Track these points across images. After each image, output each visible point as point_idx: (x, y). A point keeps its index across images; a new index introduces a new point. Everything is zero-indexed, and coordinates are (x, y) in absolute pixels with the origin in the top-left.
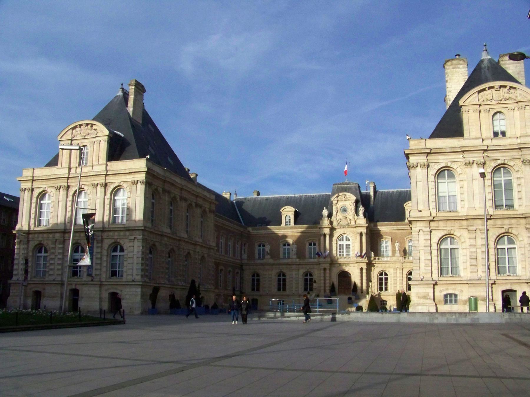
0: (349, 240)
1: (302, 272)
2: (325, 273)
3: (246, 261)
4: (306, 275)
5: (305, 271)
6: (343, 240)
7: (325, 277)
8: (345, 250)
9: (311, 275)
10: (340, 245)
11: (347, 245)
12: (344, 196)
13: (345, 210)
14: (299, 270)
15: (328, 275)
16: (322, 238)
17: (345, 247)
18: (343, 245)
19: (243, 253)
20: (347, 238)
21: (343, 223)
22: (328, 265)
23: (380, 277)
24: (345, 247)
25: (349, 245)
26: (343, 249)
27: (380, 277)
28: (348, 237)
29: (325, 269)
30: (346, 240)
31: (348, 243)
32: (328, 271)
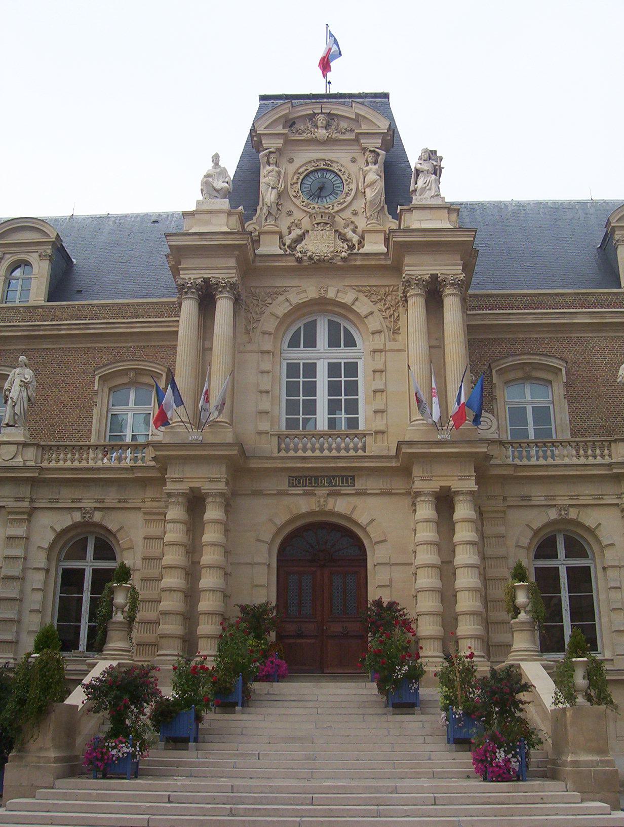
0: (351, 342)
1: (48, 526)
5: (64, 521)
6: (311, 342)
7: (193, 549)
8: (322, 397)
10: (293, 370)
11: (334, 369)
12: (321, 120)
14: (31, 513)
15: (211, 535)
17: (322, 380)
18: (311, 370)
20: (334, 328)
21: (319, 244)
22: (220, 472)
23: (542, 563)
24: (322, 380)
25: (352, 369)
26: (311, 389)
27: (542, 563)
28: (344, 323)
29: (195, 503)
30: (333, 342)
31: (342, 355)
32: (213, 513)
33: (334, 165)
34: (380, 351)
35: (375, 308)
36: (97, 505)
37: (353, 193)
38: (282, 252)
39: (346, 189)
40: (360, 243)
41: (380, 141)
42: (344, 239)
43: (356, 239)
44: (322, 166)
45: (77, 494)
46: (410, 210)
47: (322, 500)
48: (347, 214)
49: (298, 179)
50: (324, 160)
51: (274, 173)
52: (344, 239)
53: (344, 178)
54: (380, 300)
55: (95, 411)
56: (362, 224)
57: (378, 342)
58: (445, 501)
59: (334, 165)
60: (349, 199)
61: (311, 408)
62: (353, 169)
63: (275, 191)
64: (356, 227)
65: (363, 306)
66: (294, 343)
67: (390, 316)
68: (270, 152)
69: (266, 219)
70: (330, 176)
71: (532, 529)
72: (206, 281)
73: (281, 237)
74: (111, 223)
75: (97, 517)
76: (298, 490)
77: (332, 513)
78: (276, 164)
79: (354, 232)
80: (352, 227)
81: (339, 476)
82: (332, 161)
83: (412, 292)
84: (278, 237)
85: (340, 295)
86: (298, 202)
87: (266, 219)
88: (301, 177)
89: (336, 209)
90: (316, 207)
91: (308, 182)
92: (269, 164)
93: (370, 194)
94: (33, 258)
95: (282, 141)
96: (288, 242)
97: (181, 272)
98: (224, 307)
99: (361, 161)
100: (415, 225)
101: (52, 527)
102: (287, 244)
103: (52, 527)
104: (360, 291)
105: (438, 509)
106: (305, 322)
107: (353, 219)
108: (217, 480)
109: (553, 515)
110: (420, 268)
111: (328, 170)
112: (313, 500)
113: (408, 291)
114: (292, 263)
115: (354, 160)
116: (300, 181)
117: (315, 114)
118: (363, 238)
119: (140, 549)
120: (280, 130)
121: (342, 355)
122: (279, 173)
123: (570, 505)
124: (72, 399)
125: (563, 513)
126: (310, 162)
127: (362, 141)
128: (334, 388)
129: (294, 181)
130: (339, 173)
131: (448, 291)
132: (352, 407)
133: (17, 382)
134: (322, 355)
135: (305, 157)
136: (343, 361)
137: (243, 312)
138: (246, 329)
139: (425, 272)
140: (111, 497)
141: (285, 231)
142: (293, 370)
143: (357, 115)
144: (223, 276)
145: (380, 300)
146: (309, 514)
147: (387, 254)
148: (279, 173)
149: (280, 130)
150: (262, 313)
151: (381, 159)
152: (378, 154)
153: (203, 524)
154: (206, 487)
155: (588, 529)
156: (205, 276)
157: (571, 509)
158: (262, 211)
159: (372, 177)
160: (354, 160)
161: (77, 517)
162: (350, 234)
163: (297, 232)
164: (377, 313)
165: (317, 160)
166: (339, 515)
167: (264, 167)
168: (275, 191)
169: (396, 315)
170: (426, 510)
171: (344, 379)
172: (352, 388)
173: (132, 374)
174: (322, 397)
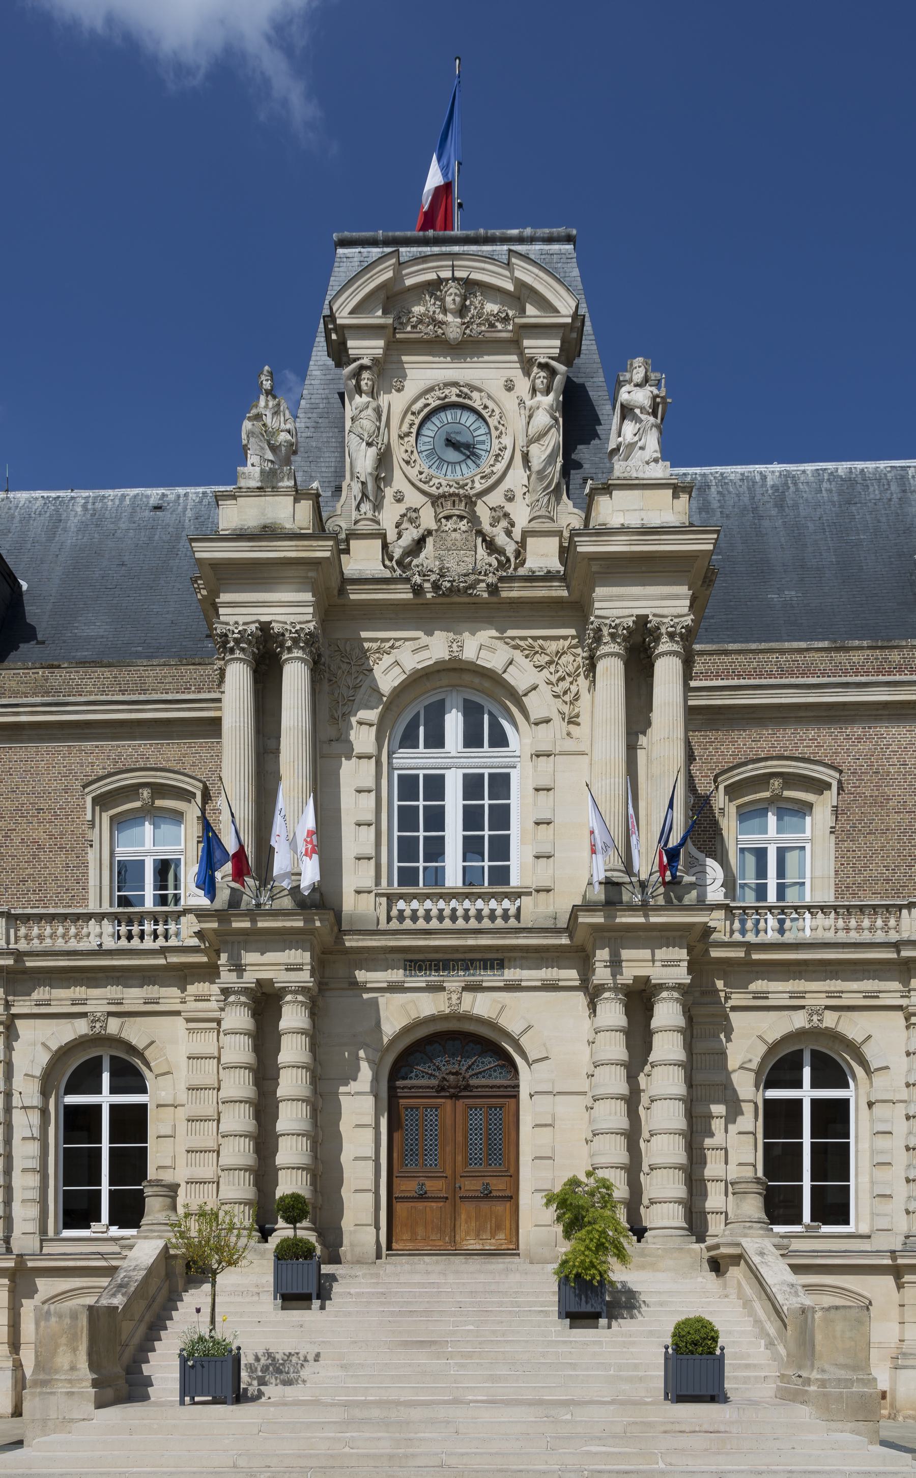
0: (499, 739)
4: (85, 1079)
5: (65, 1033)
6: (436, 740)
8: (454, 833)
9: (129, 1076)
10: (408, 786)
11: (472, 785)
17: (454, 803)
18: (436, 786)
20: (472, 713)
24: (454, 803)
25: (501, 784)
26: (436, 819)
30: (472, 739)
31: (485, 761)
33: (475, 395)
35: (540, 678)
36: (113, 1008)
37: (507, 454)
38: (387, 574)
40: (518, 554)
41: (558, 343)
42: (491, 546)
44: (454, 399)
45: (79, 992)
46: (607, 489)
47: (454, 997)
48: (496, 498)
49: (411, 425)
50: (455, 384)
51: (370, 411)
52: (491, 546)
53: (493, 422)
54: (550, 663)
55: (92, 856)
56: (521, 514)
58: (640, 999)
59: (475, 395)
60: (500, 467)
61: (436, 850)
63: (373, 451)
64: (513, 525)
65: (521, 675)
66: (409, 740)
67: (565, 693)
68: (362, 368)
69: (358, 508)
70: (468, 419)
71: (765, 1042)
73: (385, 546)
74: (79, 509)
75: (113, 1026)
76: (419, 980)
78: (373, 394)
79: (509, 533)
80: (504, 523)
81: (480, 960)
82: (473, 388)
83: (604, 649)
84: (379, 542)
85: (483, 653)
86: (412, 473)
87: (358, 508)
88: (417, 422)
89: (479, 487)
90: (444, 483)
91: (429, 430)
92: (359, 391)
95: (381, 343)
96: (397, 555)
97: (221, 611)
99: (523, 385)
100: (616, 521)
101: (44, 1044)
102: (396, 556)
103: (44, 1044)
104: (516, 647)
105: (629, 1012)
106: (427, 703)
107: (509, 508)
108: (298, 968)
109: (799, 1021)
110: (617, 604)
112: (442, 996)
113: (597, 648)
114: (404, 594)
116: (414, 430)
117: (440, 281)
118: (522, 545)
120: (377, 317)
121: (485, 761)
123: (827, 1008)
124: (51, 836)
125: (815, 1018)
126: (431, 389)
127: (526, 343)
128: (472, 818)
129: (405, 428)
130: (484, 412)
131: (665, 645)
132: (501, 848)
134: (453, 758)
135: (423, 374)
136: (486, 772)
137: (326, 687)
138: (333, 717)
139: (627, 612)
140: (133, 996)
142: (408, 786)
143: (521, 285)
144: (292, 618)
145: (550, 663)
146: (432, 1019)
147: (563, 578)
148: (378, 411)
149: (377, 317)
150: (356, 688)
151: (558, 380)
152: (553, 372)
153: (278, 1036)
154: (281, 978)
156: (264, 619)
157: (827, 1012)
159: (542, 419)
160: (509, 387)
161: (81, 1027)
162: (501, 539)
163: (411, 534)
164: (543, 687)
165: (446, 385)
166: (479, 1020)
167: (351, 399)
168: (373, 451)
169: (574, 689)
171: (489, 799)
172: (501, 817)
173: (146, 793)
174: (454, 833)
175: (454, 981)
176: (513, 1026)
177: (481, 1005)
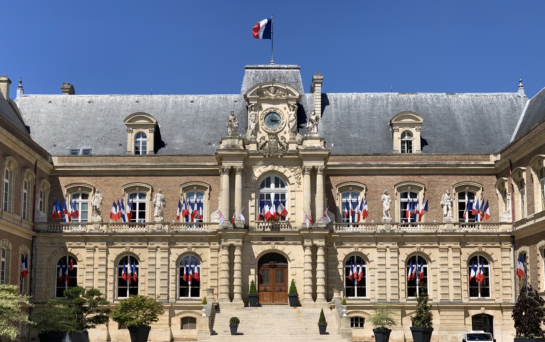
2: (231, 257)
3: (44, 227)
6: (268, 186)
11: (277, 196)
13: (273, 119)
16: (225, 179)
18: (268, 196)
19: (38, 207)
25: (283, 196)
29: (231, 249)
31: (280, 190)
34: (294, 191)
37: (285, 124)
39: (282, 122)
42: (281, 145)
43: (285, 145)
48: (282, 133)
50: (273, 108)
53: (281, 116)
56: (288, 137)
57: (293, 187)
60: (283, 126)
62: (285, 112)
70: (276, 115)
72: (232, 167)
77: (276, 250)
86: (263, 127)
89: (278, 130)
93: (292, 124)
94: (146, 131)
98: (238, 178)
99: (288, 109)
111: (275, 113)
115: (285, 109)
118: (288, 144)
119: (210, 262)
122: (256, 115)
133: (159, 198)
141: (259, 141)
148: (256, 115)
155: (365, 255)
158: (249, 132)
159: (292, 117)
163: (263, 142)
170: (308, 252)
175: (273, 243)
176: (287, 252)
177: (279, 248)
